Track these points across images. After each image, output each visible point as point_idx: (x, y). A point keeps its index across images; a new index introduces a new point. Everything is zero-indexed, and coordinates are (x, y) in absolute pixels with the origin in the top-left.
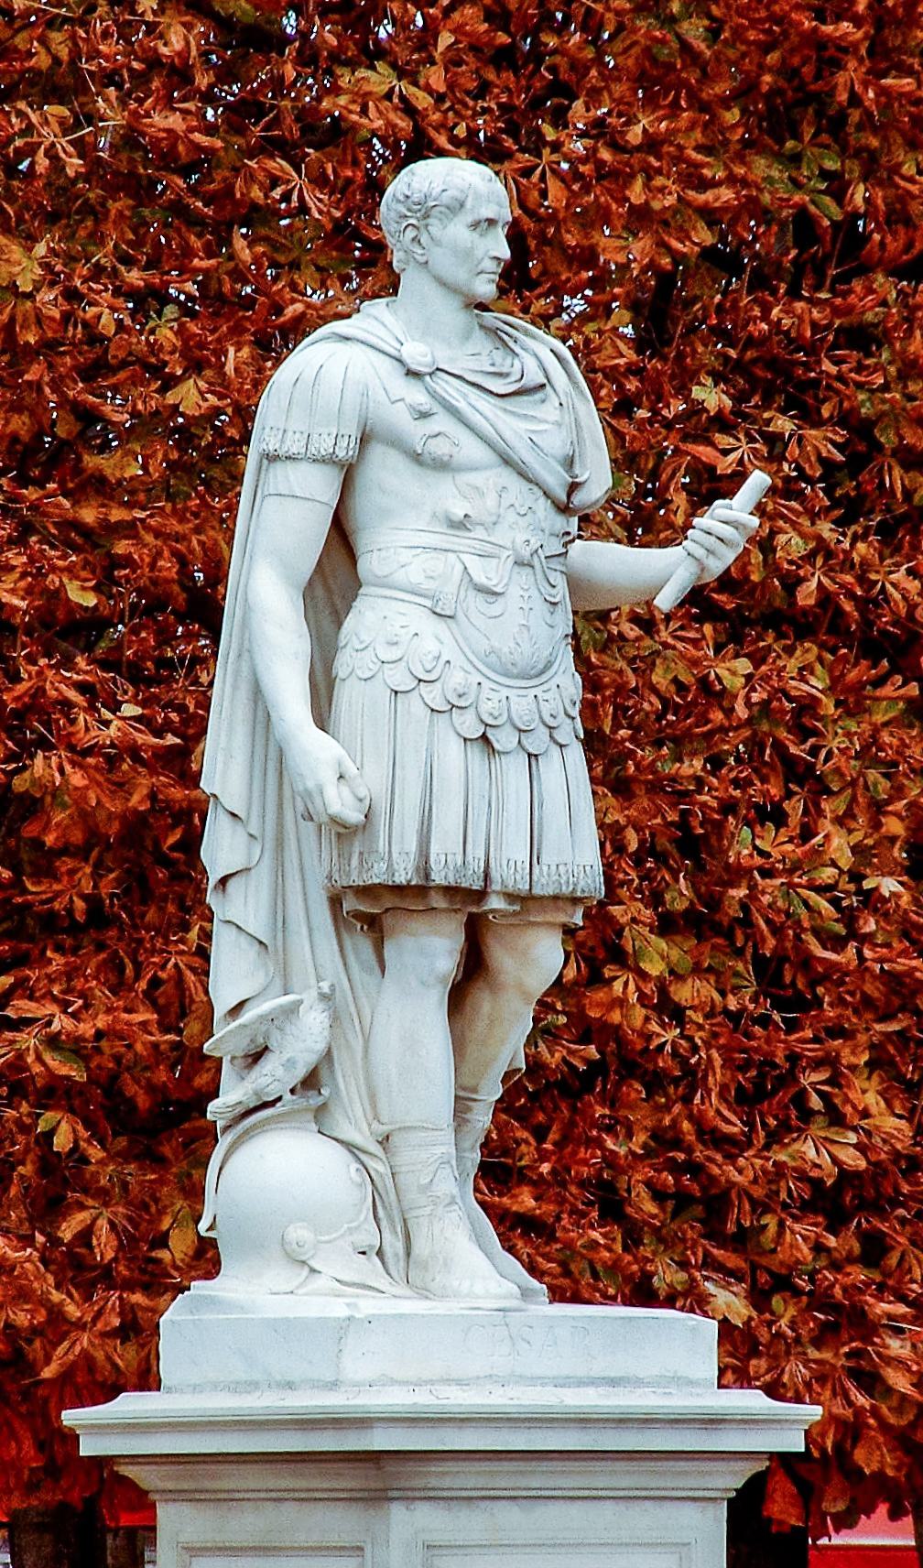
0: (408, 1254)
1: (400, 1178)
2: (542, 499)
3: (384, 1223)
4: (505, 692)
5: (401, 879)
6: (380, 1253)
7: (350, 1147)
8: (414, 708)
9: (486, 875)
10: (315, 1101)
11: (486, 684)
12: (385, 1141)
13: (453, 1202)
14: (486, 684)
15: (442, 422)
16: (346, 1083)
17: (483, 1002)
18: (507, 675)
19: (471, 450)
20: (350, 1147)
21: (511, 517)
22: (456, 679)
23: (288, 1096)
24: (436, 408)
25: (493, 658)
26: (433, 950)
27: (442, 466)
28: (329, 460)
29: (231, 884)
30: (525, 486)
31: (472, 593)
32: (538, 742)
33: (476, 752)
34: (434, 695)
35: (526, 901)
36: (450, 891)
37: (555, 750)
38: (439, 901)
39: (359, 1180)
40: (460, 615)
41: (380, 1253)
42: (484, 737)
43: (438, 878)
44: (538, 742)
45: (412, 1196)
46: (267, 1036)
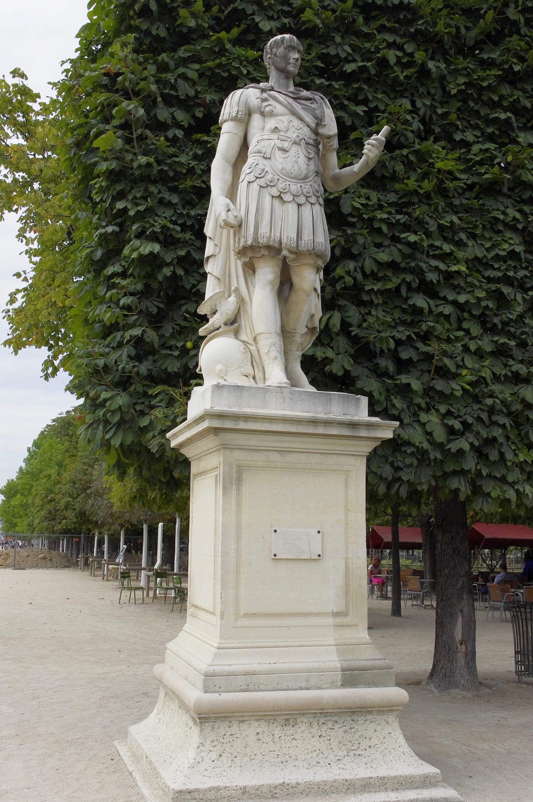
0: (265, 378)
1: (260, 352)
2: (306, 127)
3: (255, 368)
4: (288, 183)
5: (249, 243)
6: (254, 378)
7: (243, 342)
8: (255, 186)
9: (280, 243)
10: (232, 327)
11: (280, 179)
12: (255, 339)
13: (276, 358)
14: (281, 179)
15: (271, 102)
16: (243, 321)
17: (294, 297)
18: (289, 177)
19: (279, 109)
20: (243, 342)
21: (293, 129)
22: (269, 177)
23: (223, 326)
24: (269, 98)
25: (284, 171)
26: (267, 273)
27: (272, 114)
28: (235, 119)
29: (210, 260)
30: (300, 122)
31: (277, 151)
32: (302, 200)
33: (277, 202)
34: (262, 182)
35: (297, 253)
36: (269, 247)
37: (309, 206)
38: (264, 252)
39: (244, 351)
40: (272, 157)
41: (254, 378)
42: (280, 197)
43: (262, 241)
44: (302, 200)
45: (264, 358)
46: (215, 306)
